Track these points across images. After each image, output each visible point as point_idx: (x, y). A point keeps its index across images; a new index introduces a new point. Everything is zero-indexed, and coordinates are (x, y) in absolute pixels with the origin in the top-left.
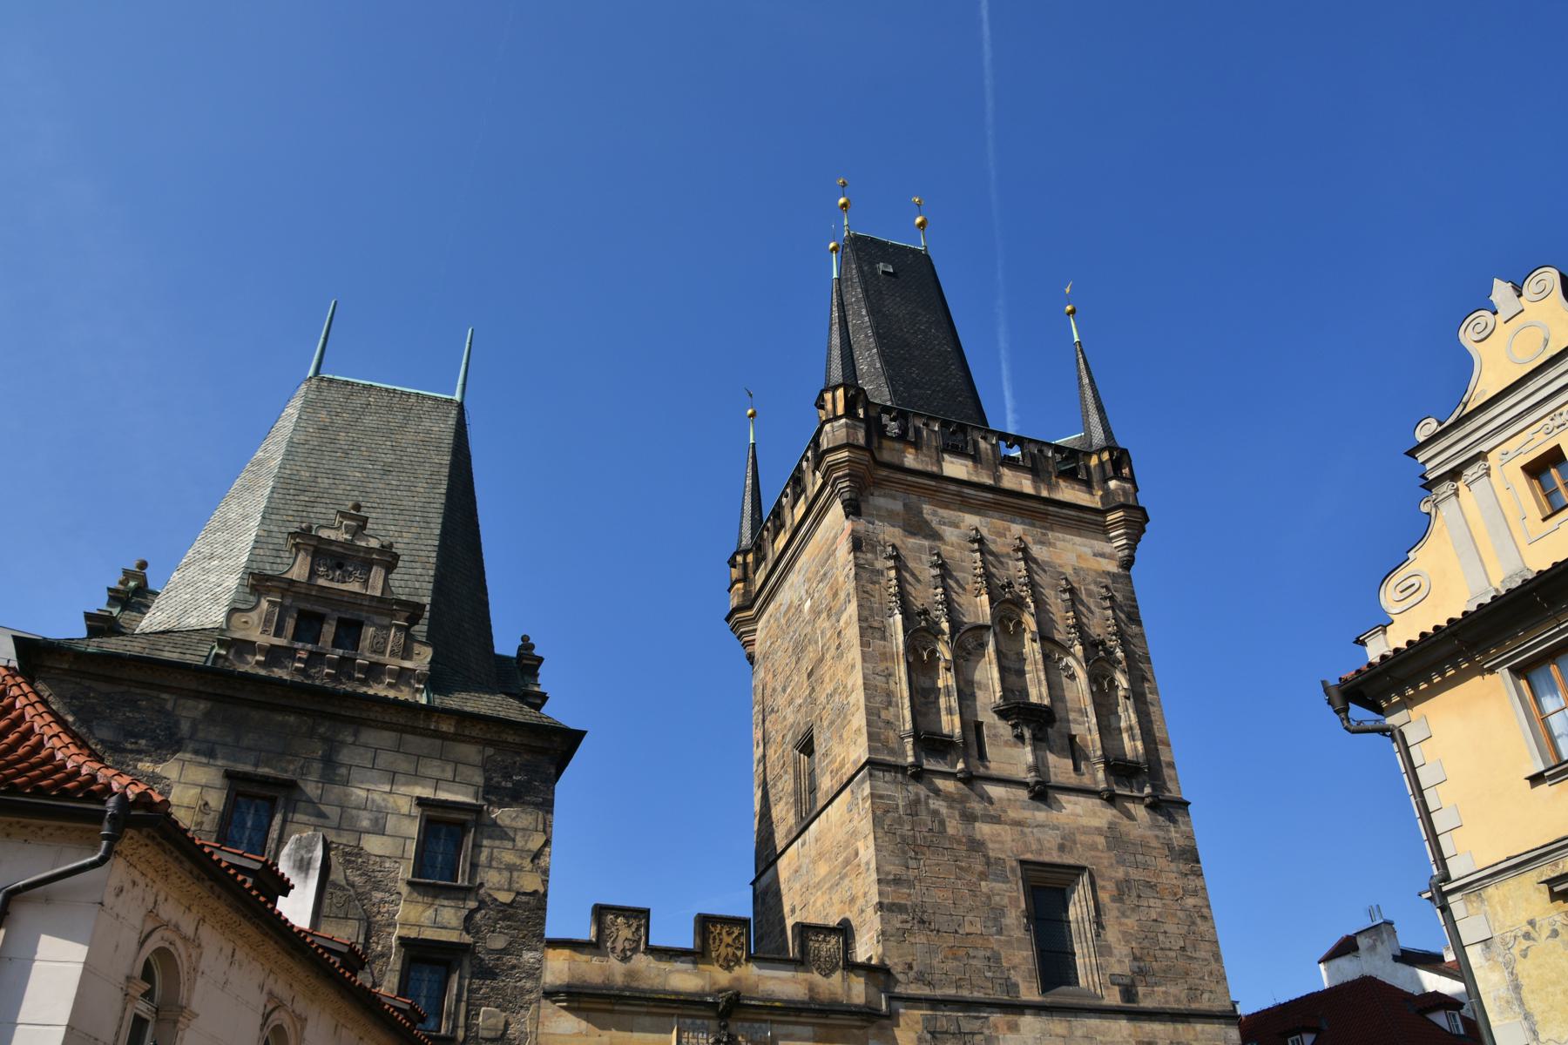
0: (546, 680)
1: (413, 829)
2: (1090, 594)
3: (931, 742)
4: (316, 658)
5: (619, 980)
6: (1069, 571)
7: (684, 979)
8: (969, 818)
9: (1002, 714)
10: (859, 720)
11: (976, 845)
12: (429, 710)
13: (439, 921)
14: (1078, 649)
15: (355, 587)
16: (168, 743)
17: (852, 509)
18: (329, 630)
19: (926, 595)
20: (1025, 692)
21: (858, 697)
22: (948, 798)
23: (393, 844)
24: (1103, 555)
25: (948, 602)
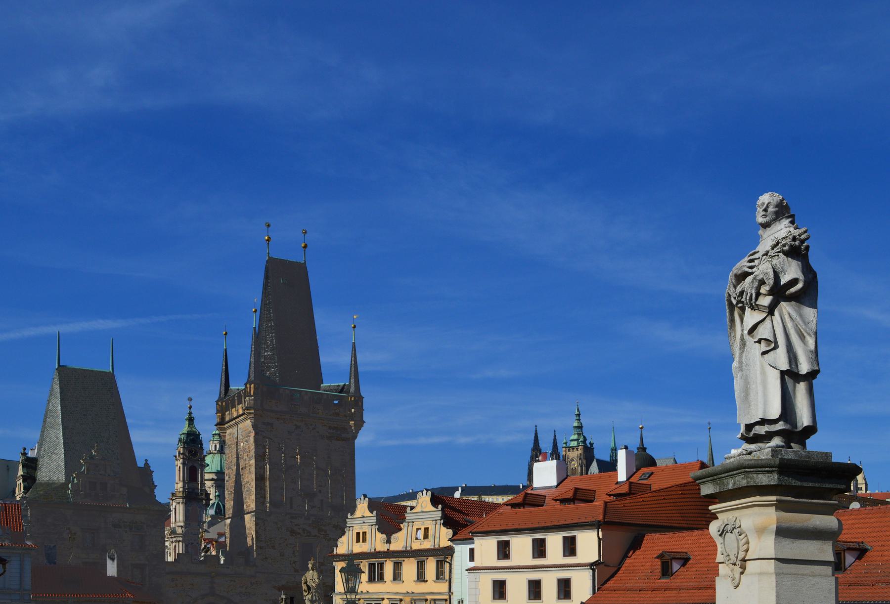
10: (253, 497)
21: (253, 489)
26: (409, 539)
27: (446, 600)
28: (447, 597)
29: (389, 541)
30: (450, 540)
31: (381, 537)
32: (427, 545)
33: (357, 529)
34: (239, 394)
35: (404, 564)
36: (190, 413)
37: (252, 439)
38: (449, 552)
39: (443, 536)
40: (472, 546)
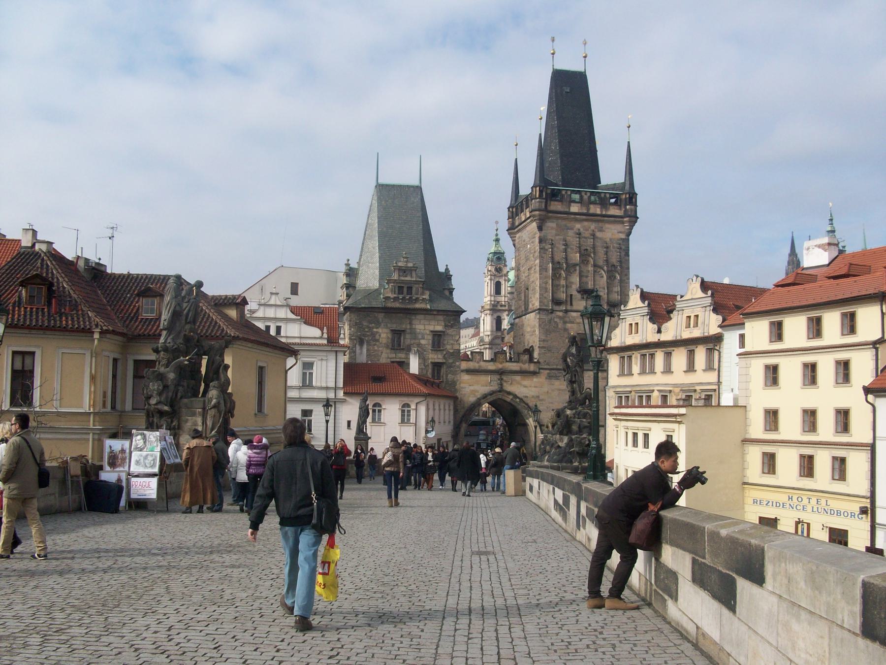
0: (454, 282)
1: (430, 337)
2: (614, 247)
3: (557, 302)
4: (404, 298)
5: (477, 368)
6: (608, 240)
7: (491, 366)
8: (565, 323)
9: (579, 292)
10: (538, 295)
11: (566, 330)
12: (431, 310)
13: (438, 358)
14: (605, 268)
15: (408, 278)
16: (378, 325)
17: (540, 228)
18: (405, 290)
19: (559, 256)
20: (587, 283)
21: (538, 288)
22: (560, 317)
23: (426, 342)
24: (620, 232)
25: (566, 258)
26: (679, 328)
27: (715, 390)
28: (715, 387)
29: (659, 331)
30: (720, 326)
31: (652, 327)
32: (696, 333)
33: (630, 320)
34: (527, 197)
35: (673, 353)
36: (497, 235)
37: (537, 240)
38: (717, 339)
39: (712, 323)
40: (741, 332)
